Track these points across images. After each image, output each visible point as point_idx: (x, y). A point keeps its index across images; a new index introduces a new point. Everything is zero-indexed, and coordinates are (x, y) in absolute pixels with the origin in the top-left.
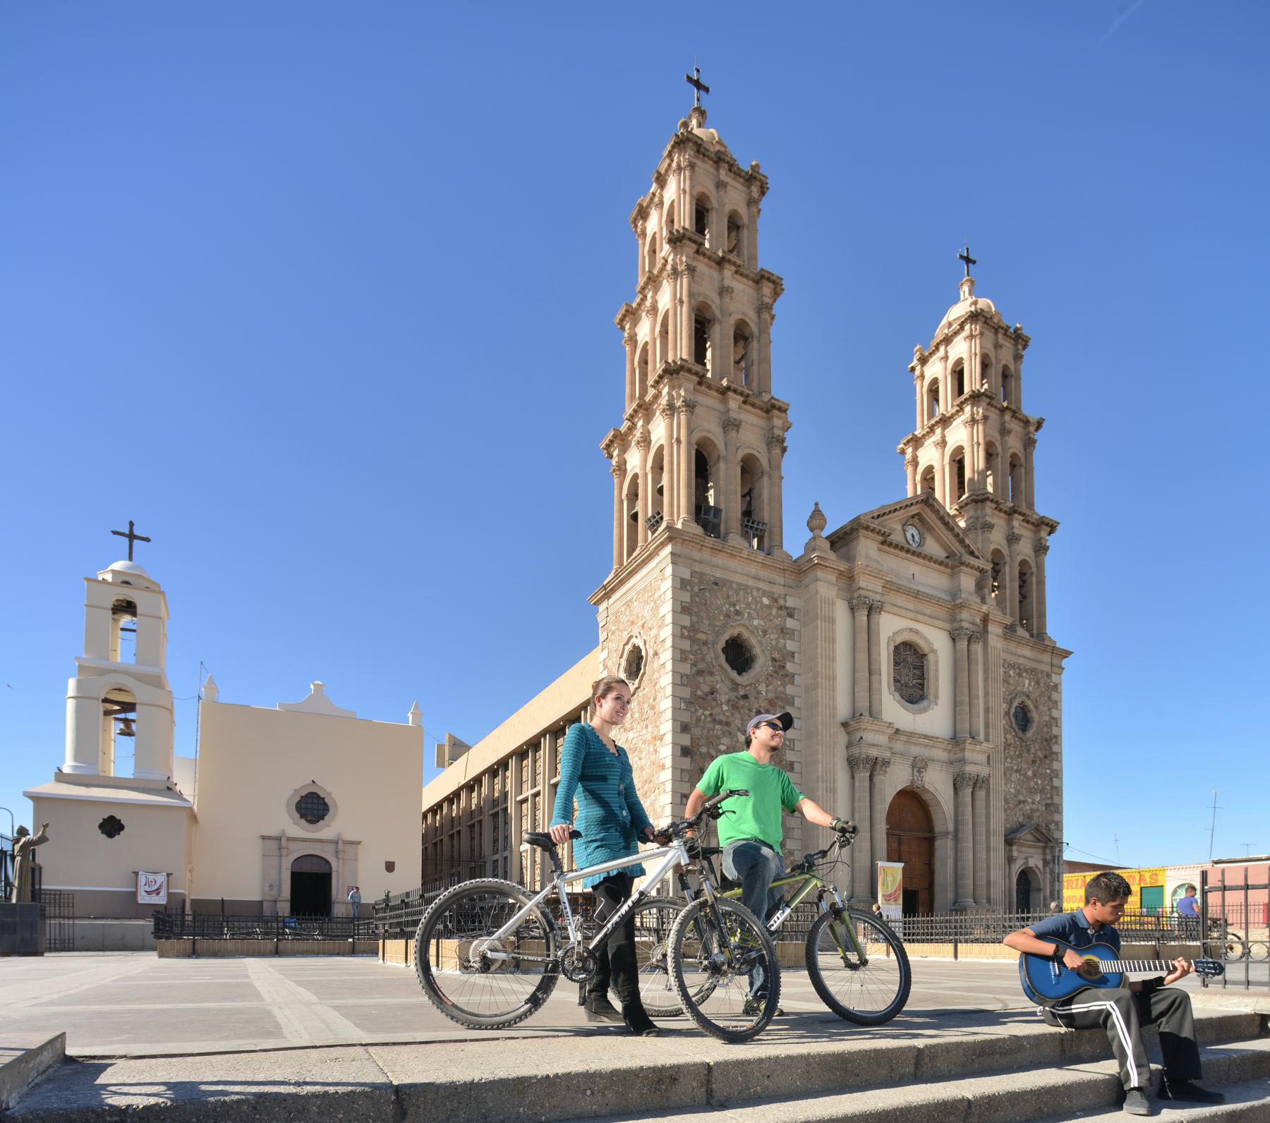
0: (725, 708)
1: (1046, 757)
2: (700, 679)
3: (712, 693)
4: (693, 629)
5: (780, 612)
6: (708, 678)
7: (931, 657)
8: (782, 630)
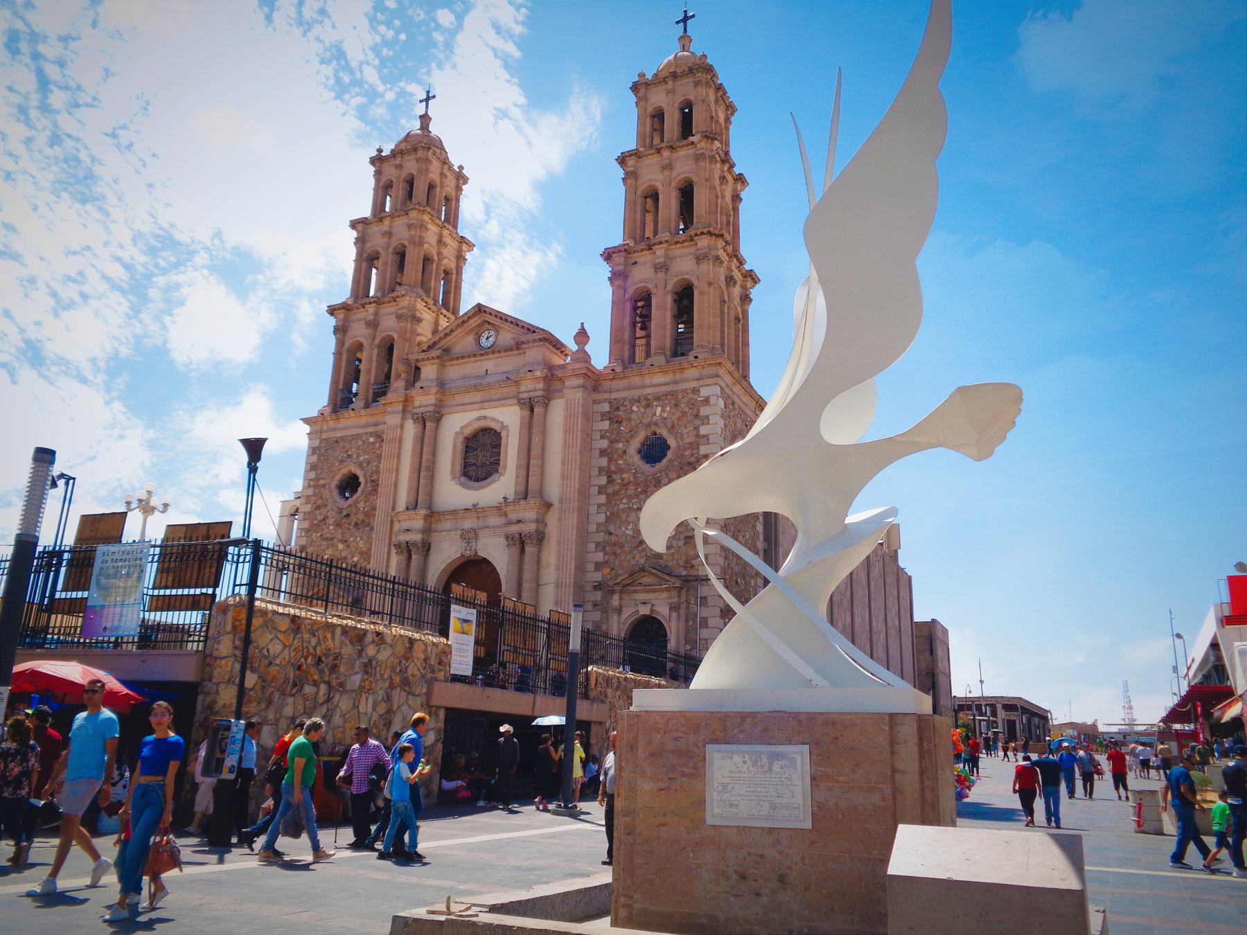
2: (318, 512)
4: (317, 479)
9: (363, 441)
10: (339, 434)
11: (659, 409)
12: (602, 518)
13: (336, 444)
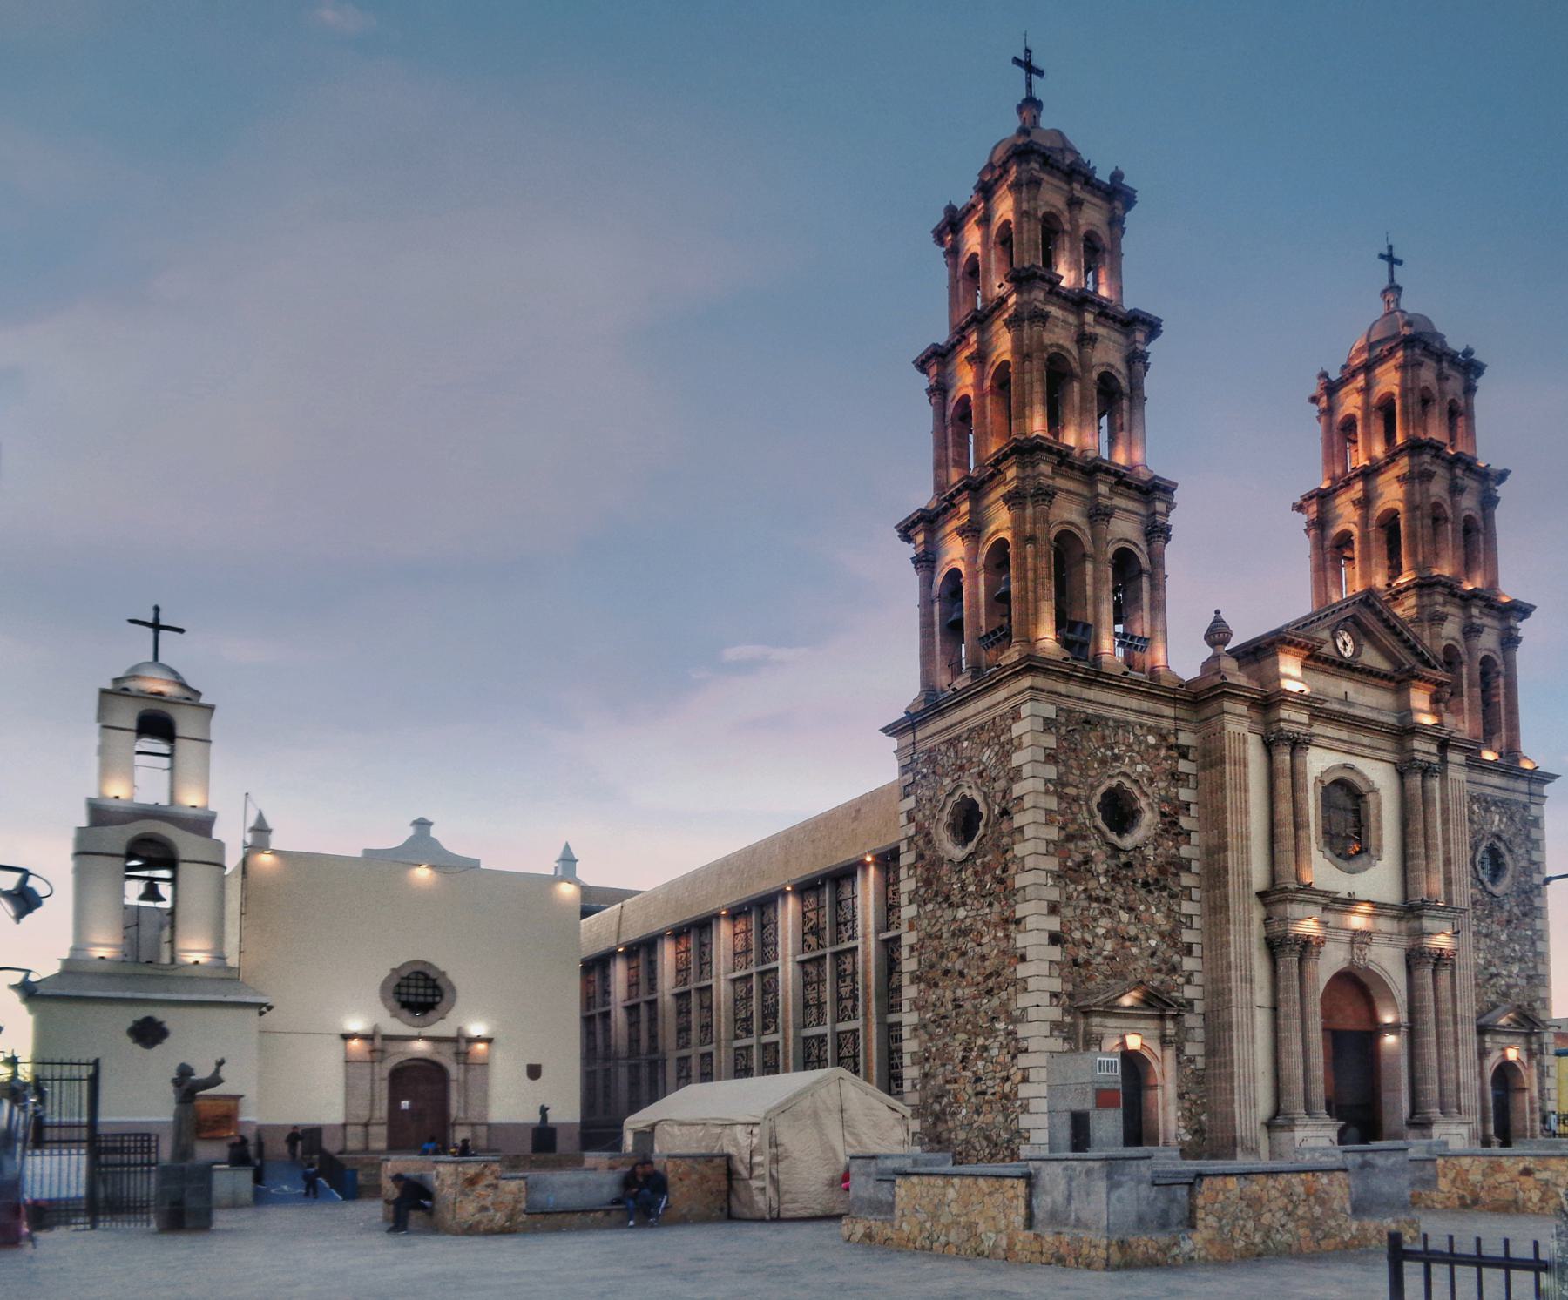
0: (1103, 880)
1: (1525, 914)
2: (1072, 846)
3: (1086, 863)
4: (1060, 782)
5: (1171, 752)
6: (1081, 844)
7: (1371, 797)
8: (1173, 775)
10: (1091, 710)
13: (1087, 727)
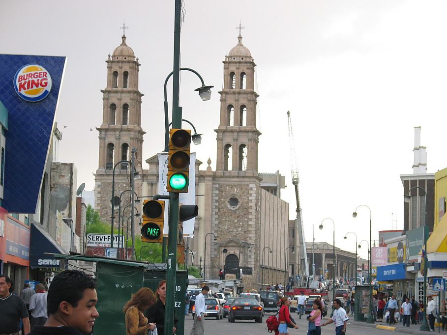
1: (245, 214)
2: (103, 210)
4: (101, 197)
6: (105, 209)
9: (121, 186)
11: (236, 190)
12: (217, 222)
